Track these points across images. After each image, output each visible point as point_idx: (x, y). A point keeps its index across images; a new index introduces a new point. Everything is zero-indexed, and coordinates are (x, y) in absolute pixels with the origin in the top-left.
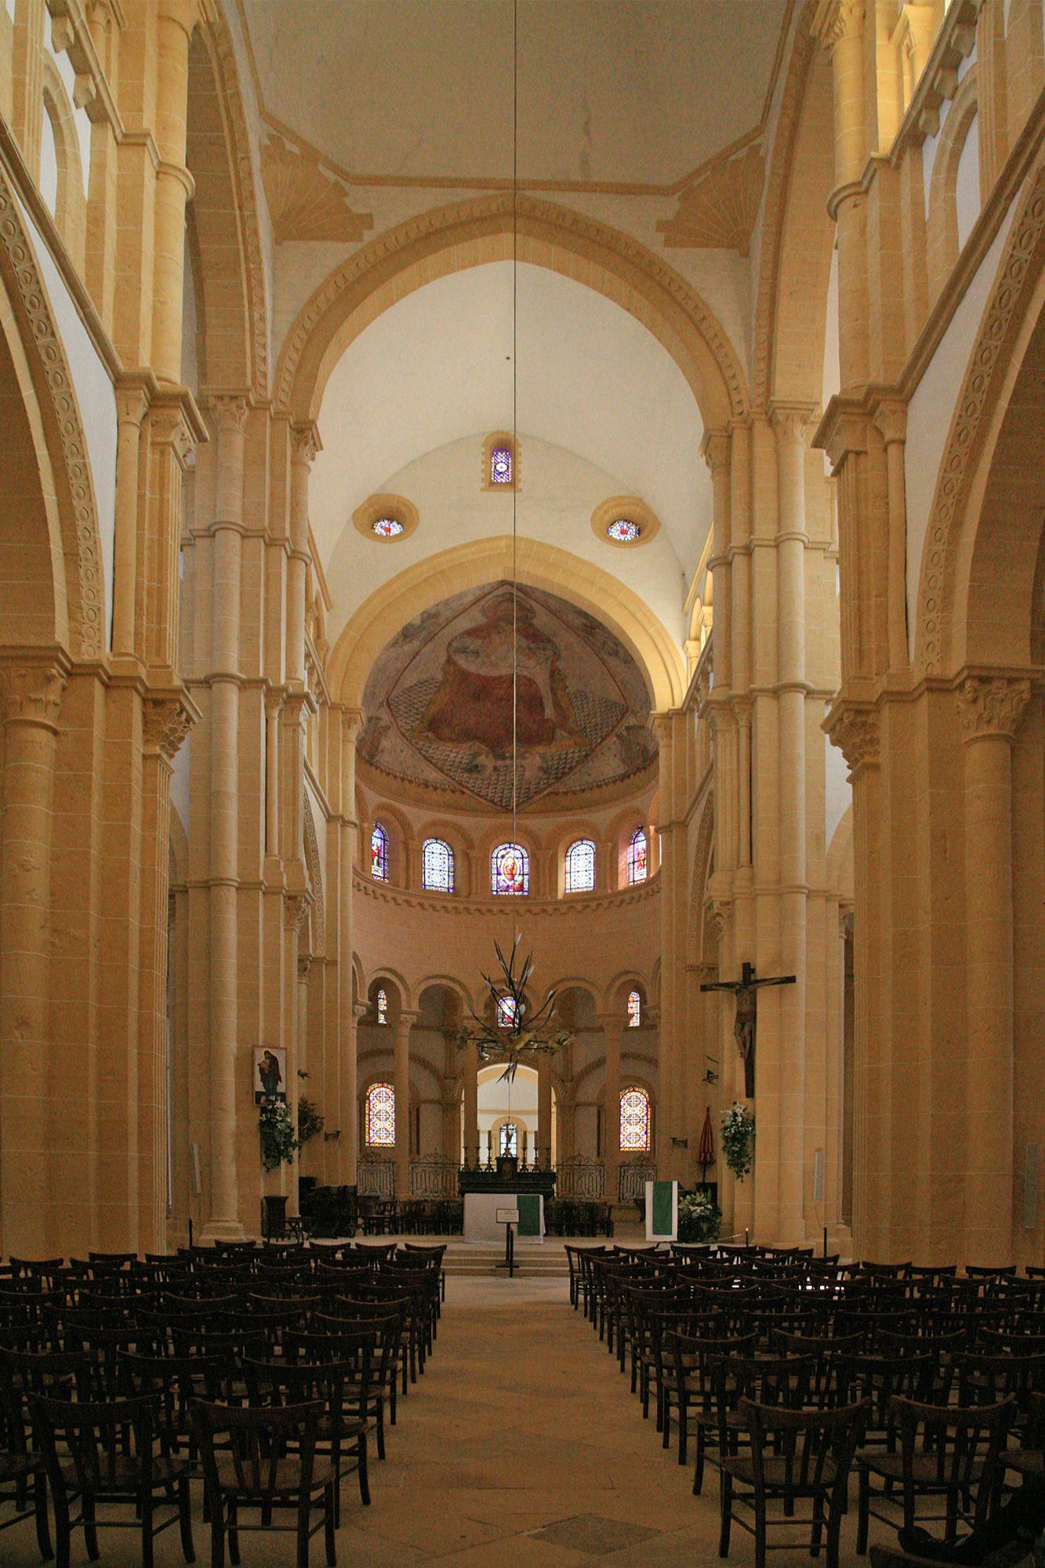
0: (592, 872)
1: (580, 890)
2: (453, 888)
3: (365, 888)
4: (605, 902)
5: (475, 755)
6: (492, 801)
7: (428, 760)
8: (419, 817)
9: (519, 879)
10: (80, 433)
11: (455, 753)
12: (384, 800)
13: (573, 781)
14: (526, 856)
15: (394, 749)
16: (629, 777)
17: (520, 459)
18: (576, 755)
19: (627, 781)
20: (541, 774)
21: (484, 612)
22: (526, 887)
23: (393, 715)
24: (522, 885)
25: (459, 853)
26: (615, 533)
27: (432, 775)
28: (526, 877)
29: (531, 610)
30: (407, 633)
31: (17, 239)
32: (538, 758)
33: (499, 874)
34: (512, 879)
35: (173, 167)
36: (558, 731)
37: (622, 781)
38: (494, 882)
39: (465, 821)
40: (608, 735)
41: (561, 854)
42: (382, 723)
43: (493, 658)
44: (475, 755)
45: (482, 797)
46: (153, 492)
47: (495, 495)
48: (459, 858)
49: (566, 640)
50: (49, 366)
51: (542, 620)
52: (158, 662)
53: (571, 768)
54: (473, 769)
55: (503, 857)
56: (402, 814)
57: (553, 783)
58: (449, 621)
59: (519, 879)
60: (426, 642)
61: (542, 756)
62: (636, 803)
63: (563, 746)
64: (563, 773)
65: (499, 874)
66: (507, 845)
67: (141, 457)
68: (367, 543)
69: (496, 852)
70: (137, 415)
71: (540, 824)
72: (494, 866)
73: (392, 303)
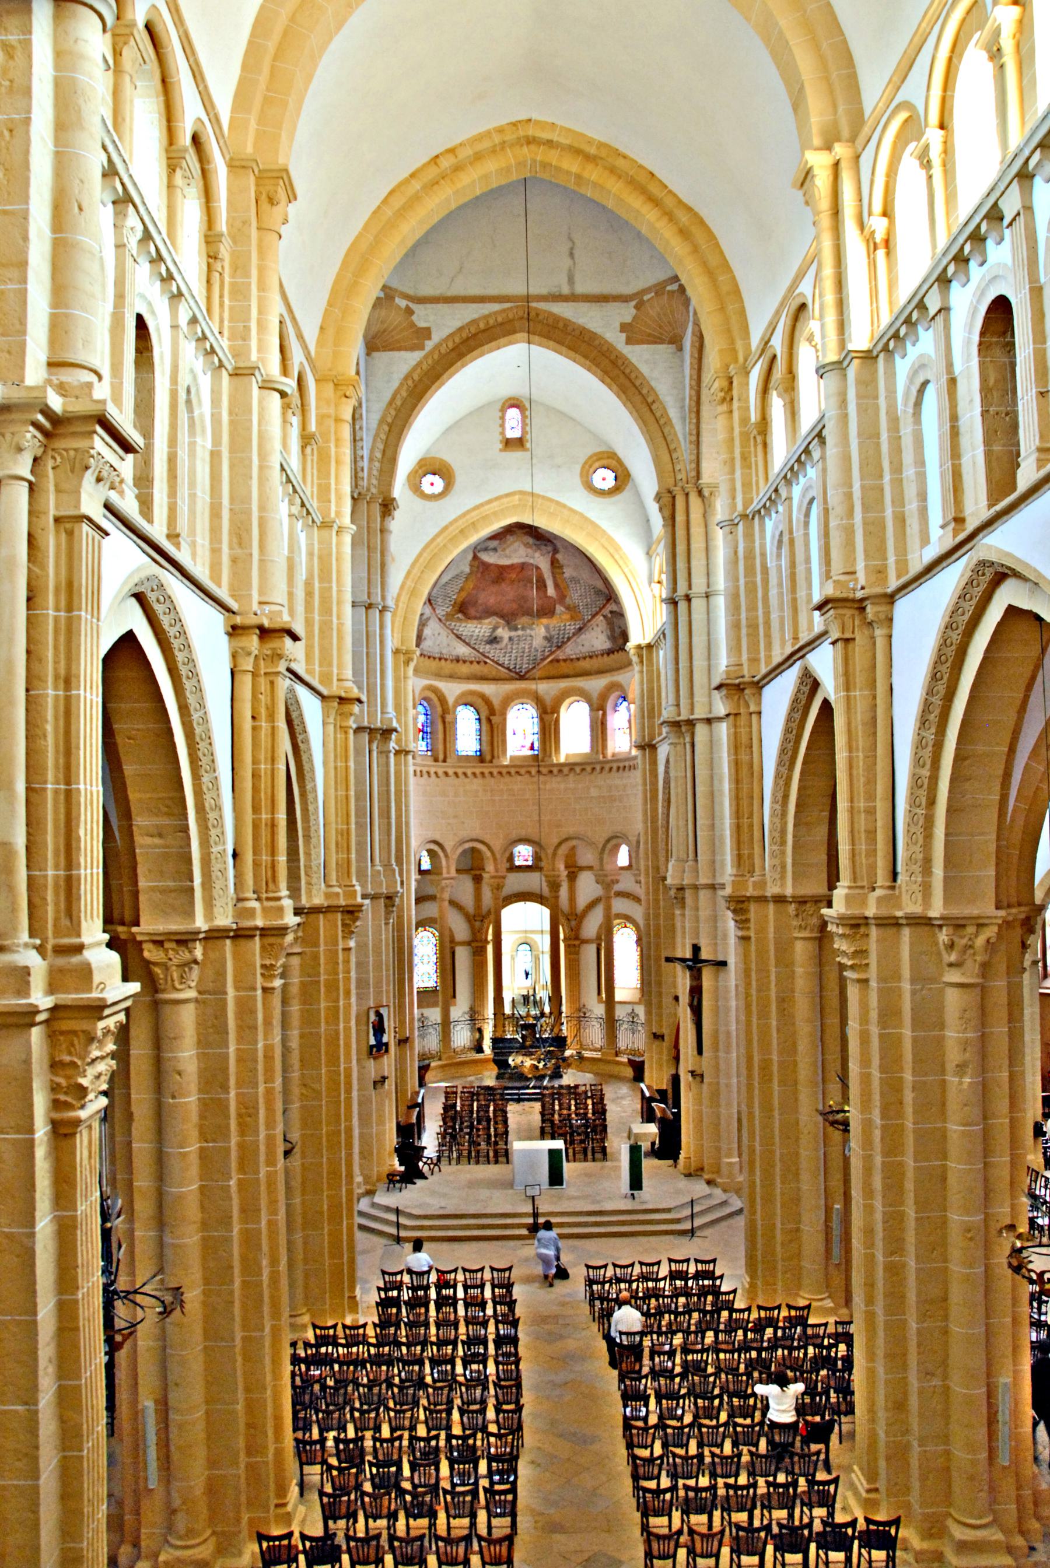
7: (459, 637)
13: (570, 650)
18: (571, 628)
20: (545, 643)
22: (536, 746)
27: (462, 650)
39: (488, 689)
40: (597, 614)
53: (569, 639)
54: (493, 640)
71: (546, 688)
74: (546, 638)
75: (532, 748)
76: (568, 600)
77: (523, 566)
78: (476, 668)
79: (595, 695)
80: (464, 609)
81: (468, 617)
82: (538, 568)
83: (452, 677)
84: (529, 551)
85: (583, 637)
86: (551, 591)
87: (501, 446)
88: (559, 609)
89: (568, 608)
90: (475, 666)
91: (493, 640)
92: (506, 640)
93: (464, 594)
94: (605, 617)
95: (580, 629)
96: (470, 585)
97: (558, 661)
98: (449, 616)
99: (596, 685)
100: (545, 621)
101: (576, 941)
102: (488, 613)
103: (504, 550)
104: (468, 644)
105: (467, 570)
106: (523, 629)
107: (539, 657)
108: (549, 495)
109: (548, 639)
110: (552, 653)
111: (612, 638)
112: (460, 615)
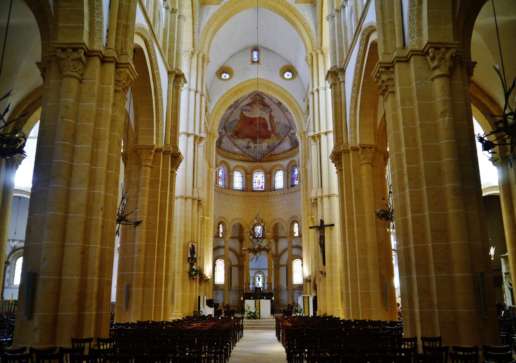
0: (283, 182)
1: (279, 188)
2: (243, 188)
3: (219, 191)
4: (286, 192)
5: (249, 143)
6: (253, 158)
7: (235, 145)
8: (233, 164)
9: (261, 184)
10: (162, 91)
11: (242, 143)
12: (223, 159)
13: (277, 151)
14: (263, 176)
15: (227, 143)
16: (292, 149)
17: (260, 54)
19: (292, 151)
20: (267, 149)
21: (251, 99)
22: (263, 187)
23: (226, 131)
24: (262, 186)
25: (244, 176)
26: (286, 75)
28: (264, 184)
29: (264, 98)
30: (230, 107)
31: (152, 47)
32: (266, 143)
33: (255, 183)
34: (259, 184)
35: (183, 16)
36: (272, 134)
37: (290, 151)
38: (254, 186)
39: (246, 165)
40: (286, 136)
41: (273, 175)
42: (223, 134)
43: (254, 112)
44: (249, 143)
45: (250, 156)
46: (175, 100)
47: (255, 66)
48: (244, 178)
49: (274, 107)
50: (157, 77)
51: (267, 101)
52: (174, 146)
53: (276, 147)
55: (257, 177)
56: (228, 163)
57: (271, 152)
58: (241, 102)
59: (261, 184)
60: (235, 109)
61: (268, 143)
62: (295, 158)
63: (273, 140)
64: (274, 148)
65: (255, 183)
66: (257, 173)
67: (173, 90)
68: (220, 81)
69: (255, 175)
70: (172, 81)
71: (267, 165)
72: (254, 180)
73: (228, 20)
74: (267, 147)
75: (262, 188)
76: (276, 132)
77: (260, 118)
78: (241, 157)
79: (285, 166)
80: (237, 134)
81: (239, 138)
82: (264, 119)
83: (232, 159)
84: (261, 111)
85: (281, 146)
86: (269, 128)
87: (251, 63)
88: (273, 135)
89: (275, 135)
90: (241, 156)
91: (248, 147)
92: (253, 148)
93: (237, 129)
94: (289, 136)
95: (280, 142)
96: (240, 125)
97: (272, 155)
98: (232, 136)
99: (285, 163)
100: (267, 140)
101: (277, 267)
102: (247, 137)
103: (252, 111)
104: (239, 148)
105: (239, 118)
106: (259, 143)
107: (265, 154)
108: (268, 79)
109: (268, 147)
110: (270, 152)
111: (292, 144)
112: (236, 137)
